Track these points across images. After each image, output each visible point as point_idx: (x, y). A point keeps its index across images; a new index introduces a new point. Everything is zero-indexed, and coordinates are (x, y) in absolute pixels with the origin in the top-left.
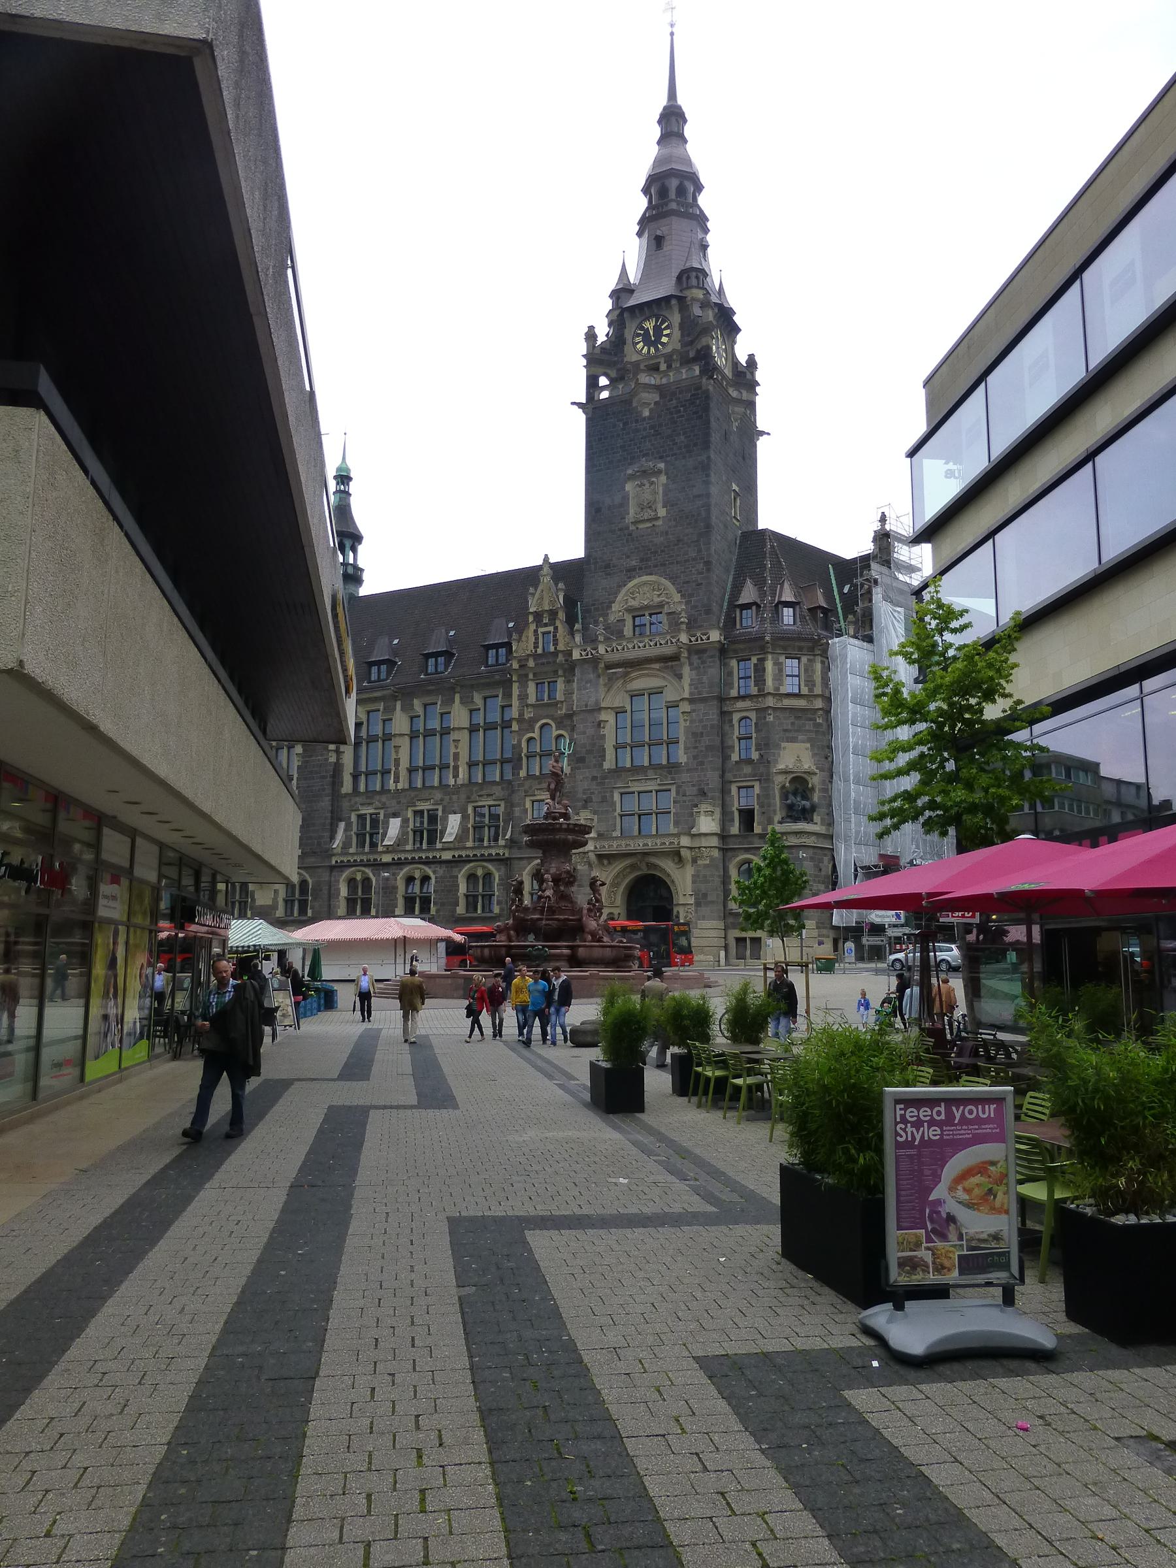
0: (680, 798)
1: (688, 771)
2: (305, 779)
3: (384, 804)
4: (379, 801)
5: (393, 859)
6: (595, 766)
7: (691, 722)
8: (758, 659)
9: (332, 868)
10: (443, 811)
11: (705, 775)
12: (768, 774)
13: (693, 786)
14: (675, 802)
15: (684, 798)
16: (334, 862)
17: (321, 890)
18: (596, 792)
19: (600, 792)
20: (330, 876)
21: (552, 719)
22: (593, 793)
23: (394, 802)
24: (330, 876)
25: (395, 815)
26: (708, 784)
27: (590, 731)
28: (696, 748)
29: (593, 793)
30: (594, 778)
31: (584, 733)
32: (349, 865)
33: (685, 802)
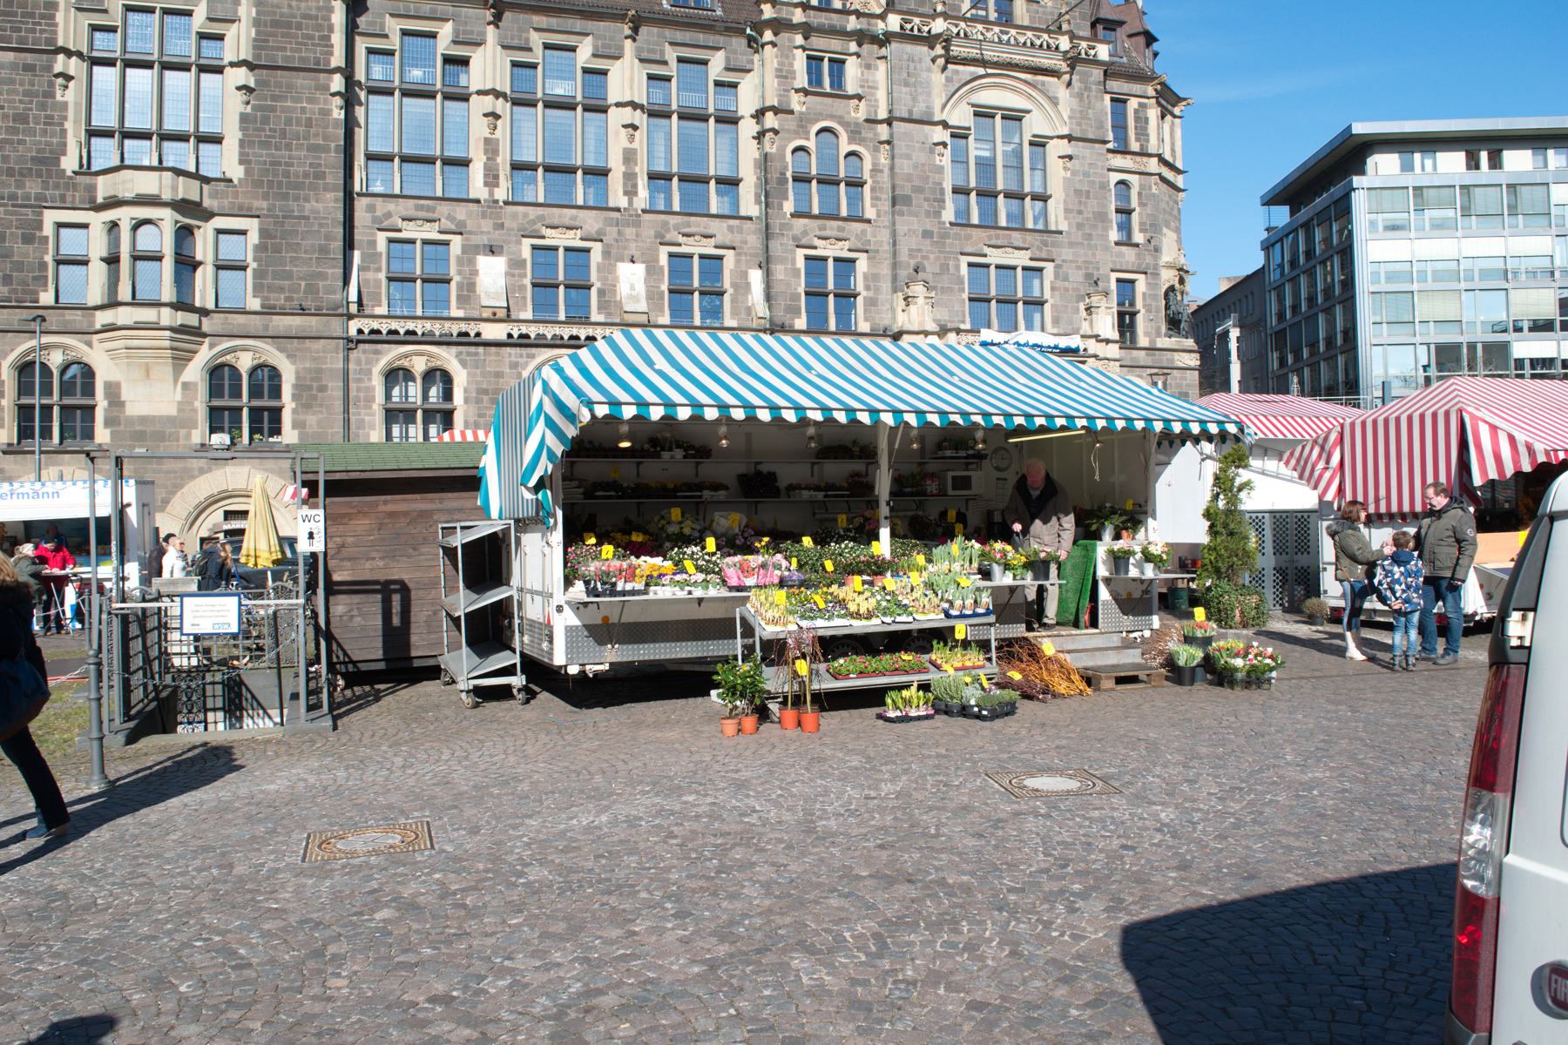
0: (1059, 284)
1: (1071, 245)
2: (265, 145)
3: (462, 224)
4: (450, 218)
5: (510, 336)
6: (928, 214)
7: (1074, 173)
8: (1141, 105)
9: (351, 343)
10: (606, 254)
11: (1094, 255)
12: (1156, 267)
13: (1079, 268)
14: (1053, 289)
15: (1066, 284)
16: (353, 332)
17: (323, 389)
18: (932, 256)
19: (937, 259)
20: (347, 360)
21: (839, 123)
22: (924, 257)
23: (487, 225)
24: (347, 360)
25: (492, 251)
26: (1098, 269)
27: (920, 157)
28: (1080, 212)
29: (924, 257)
30: (927, 234)
31: (908, 157)
32: (393, 338)
33: (1066, 290)
